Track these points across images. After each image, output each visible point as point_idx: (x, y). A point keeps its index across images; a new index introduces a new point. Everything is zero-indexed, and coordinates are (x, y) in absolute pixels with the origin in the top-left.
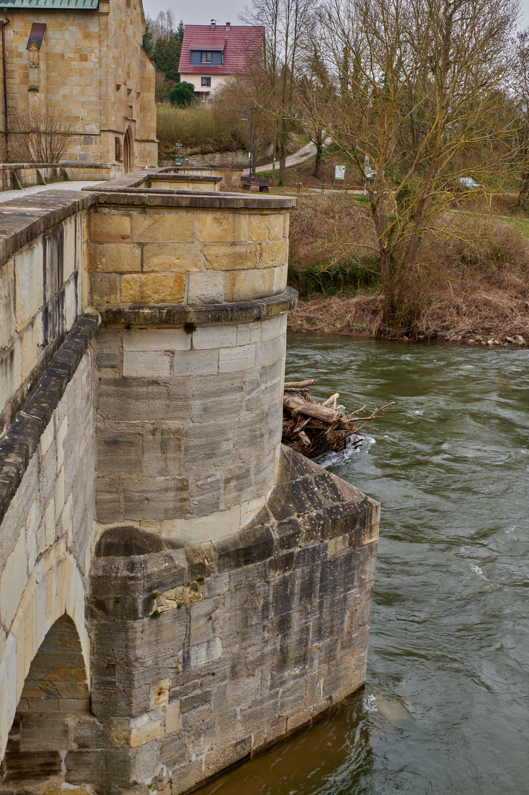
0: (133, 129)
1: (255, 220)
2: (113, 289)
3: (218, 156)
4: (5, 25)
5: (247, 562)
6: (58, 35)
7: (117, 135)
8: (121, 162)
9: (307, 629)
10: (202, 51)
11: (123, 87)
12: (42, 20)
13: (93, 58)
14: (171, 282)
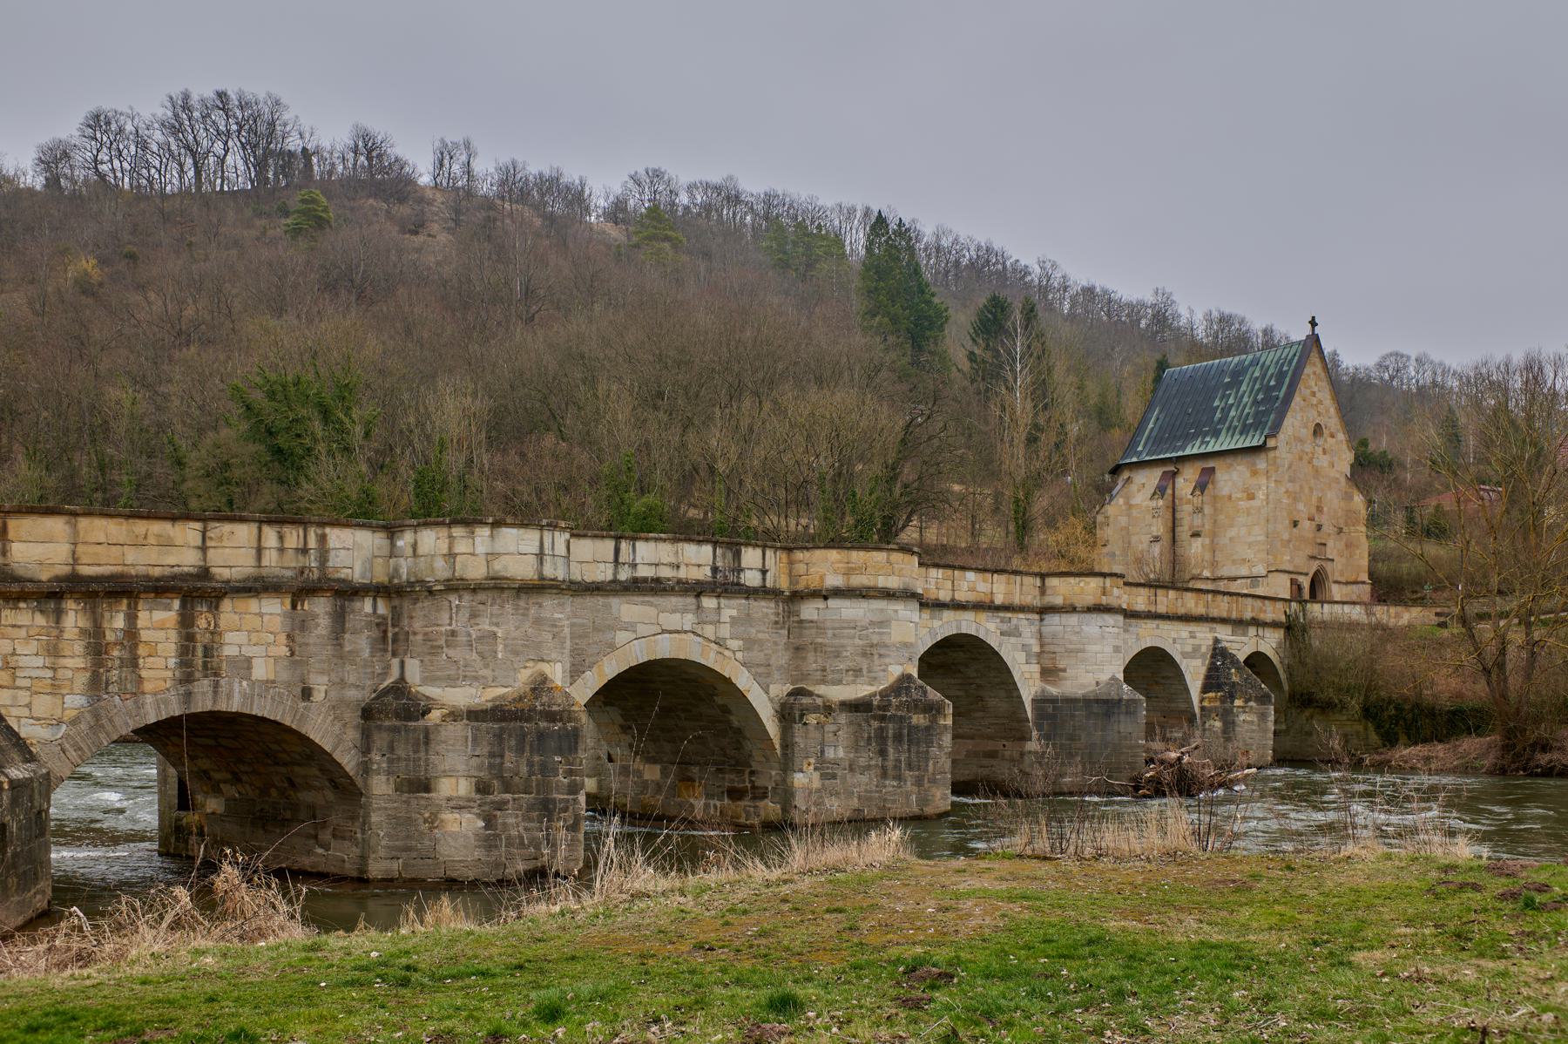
2: (797, 583)
5: (856, 711)
6: (1226, 477)
7: (1294, 576)
9: (900, 761)
12: (1210, 464)
13: (1261, 495)
14: (817, 579)
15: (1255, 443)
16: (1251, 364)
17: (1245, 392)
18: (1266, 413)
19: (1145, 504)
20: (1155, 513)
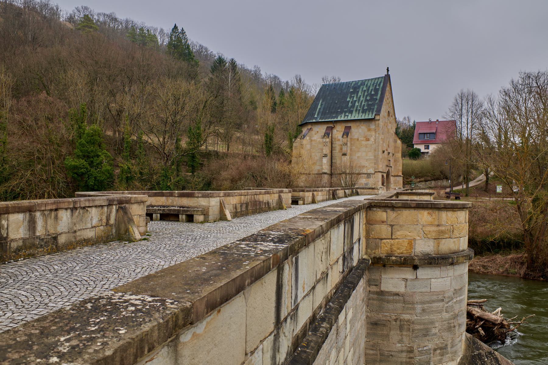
0: (390, 170)
1: (450, 214)
2: (377, 247)
3: (433, 182)
4: (333, 128)
6: (356, 131)
7: (383, 174)
8: (385, 186)
10: (425, 133)
11: (386, 151)
12: (349, 125)
13: (372, 139)
15: (370, 117)
16: (361, 84)
17: (361, 96)
18: (373, 105)
19: (318, 140)
20: (325, 144)
